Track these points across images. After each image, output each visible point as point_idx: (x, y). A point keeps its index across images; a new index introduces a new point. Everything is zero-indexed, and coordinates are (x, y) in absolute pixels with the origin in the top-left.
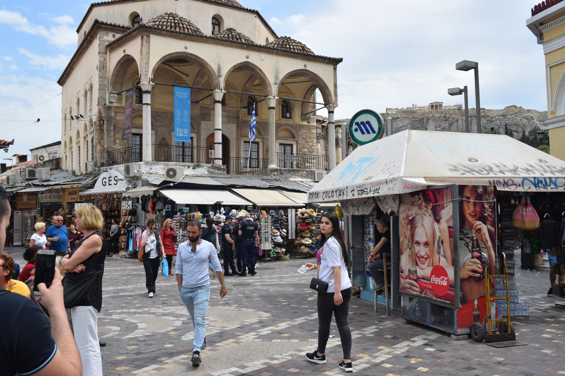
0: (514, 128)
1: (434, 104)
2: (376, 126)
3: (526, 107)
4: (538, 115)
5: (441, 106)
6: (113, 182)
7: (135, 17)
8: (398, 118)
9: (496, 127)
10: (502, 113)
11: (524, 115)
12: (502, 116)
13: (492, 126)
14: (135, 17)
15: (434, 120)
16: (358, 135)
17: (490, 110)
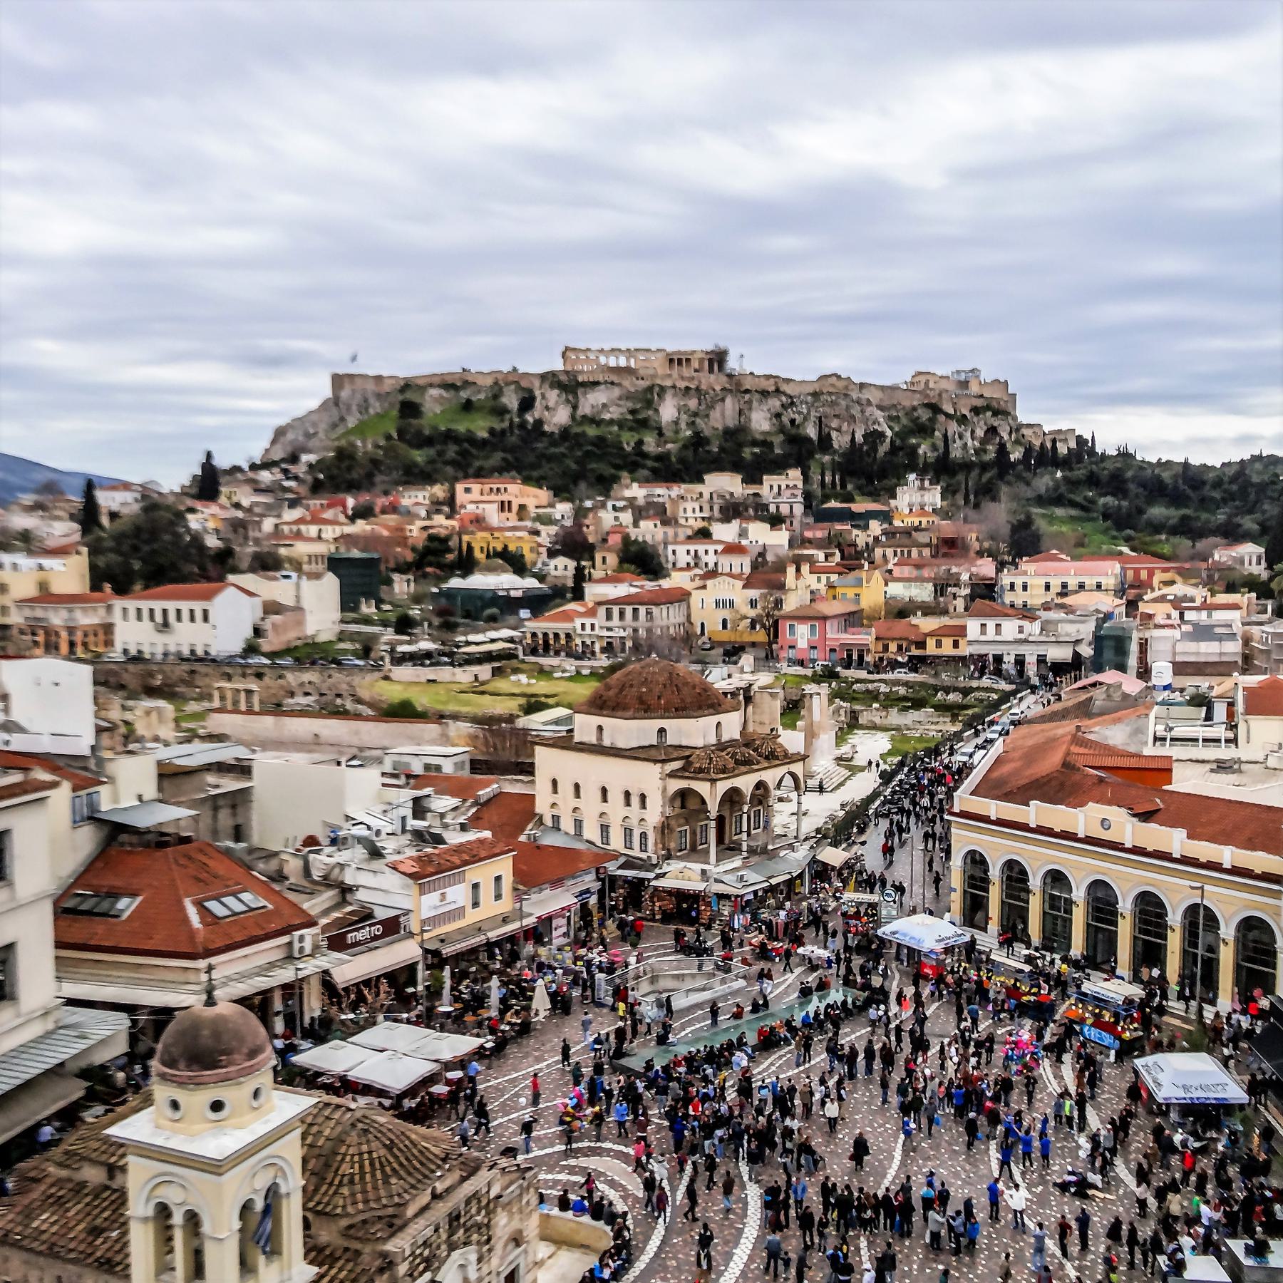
0: (834, 424)
5: (688, 360)
7: (662, 731)
9: (799, 419)
10: (810, 389)
11: (855, 395)
13: (792, 416)
14: (662, 731)
17: (788, 381)
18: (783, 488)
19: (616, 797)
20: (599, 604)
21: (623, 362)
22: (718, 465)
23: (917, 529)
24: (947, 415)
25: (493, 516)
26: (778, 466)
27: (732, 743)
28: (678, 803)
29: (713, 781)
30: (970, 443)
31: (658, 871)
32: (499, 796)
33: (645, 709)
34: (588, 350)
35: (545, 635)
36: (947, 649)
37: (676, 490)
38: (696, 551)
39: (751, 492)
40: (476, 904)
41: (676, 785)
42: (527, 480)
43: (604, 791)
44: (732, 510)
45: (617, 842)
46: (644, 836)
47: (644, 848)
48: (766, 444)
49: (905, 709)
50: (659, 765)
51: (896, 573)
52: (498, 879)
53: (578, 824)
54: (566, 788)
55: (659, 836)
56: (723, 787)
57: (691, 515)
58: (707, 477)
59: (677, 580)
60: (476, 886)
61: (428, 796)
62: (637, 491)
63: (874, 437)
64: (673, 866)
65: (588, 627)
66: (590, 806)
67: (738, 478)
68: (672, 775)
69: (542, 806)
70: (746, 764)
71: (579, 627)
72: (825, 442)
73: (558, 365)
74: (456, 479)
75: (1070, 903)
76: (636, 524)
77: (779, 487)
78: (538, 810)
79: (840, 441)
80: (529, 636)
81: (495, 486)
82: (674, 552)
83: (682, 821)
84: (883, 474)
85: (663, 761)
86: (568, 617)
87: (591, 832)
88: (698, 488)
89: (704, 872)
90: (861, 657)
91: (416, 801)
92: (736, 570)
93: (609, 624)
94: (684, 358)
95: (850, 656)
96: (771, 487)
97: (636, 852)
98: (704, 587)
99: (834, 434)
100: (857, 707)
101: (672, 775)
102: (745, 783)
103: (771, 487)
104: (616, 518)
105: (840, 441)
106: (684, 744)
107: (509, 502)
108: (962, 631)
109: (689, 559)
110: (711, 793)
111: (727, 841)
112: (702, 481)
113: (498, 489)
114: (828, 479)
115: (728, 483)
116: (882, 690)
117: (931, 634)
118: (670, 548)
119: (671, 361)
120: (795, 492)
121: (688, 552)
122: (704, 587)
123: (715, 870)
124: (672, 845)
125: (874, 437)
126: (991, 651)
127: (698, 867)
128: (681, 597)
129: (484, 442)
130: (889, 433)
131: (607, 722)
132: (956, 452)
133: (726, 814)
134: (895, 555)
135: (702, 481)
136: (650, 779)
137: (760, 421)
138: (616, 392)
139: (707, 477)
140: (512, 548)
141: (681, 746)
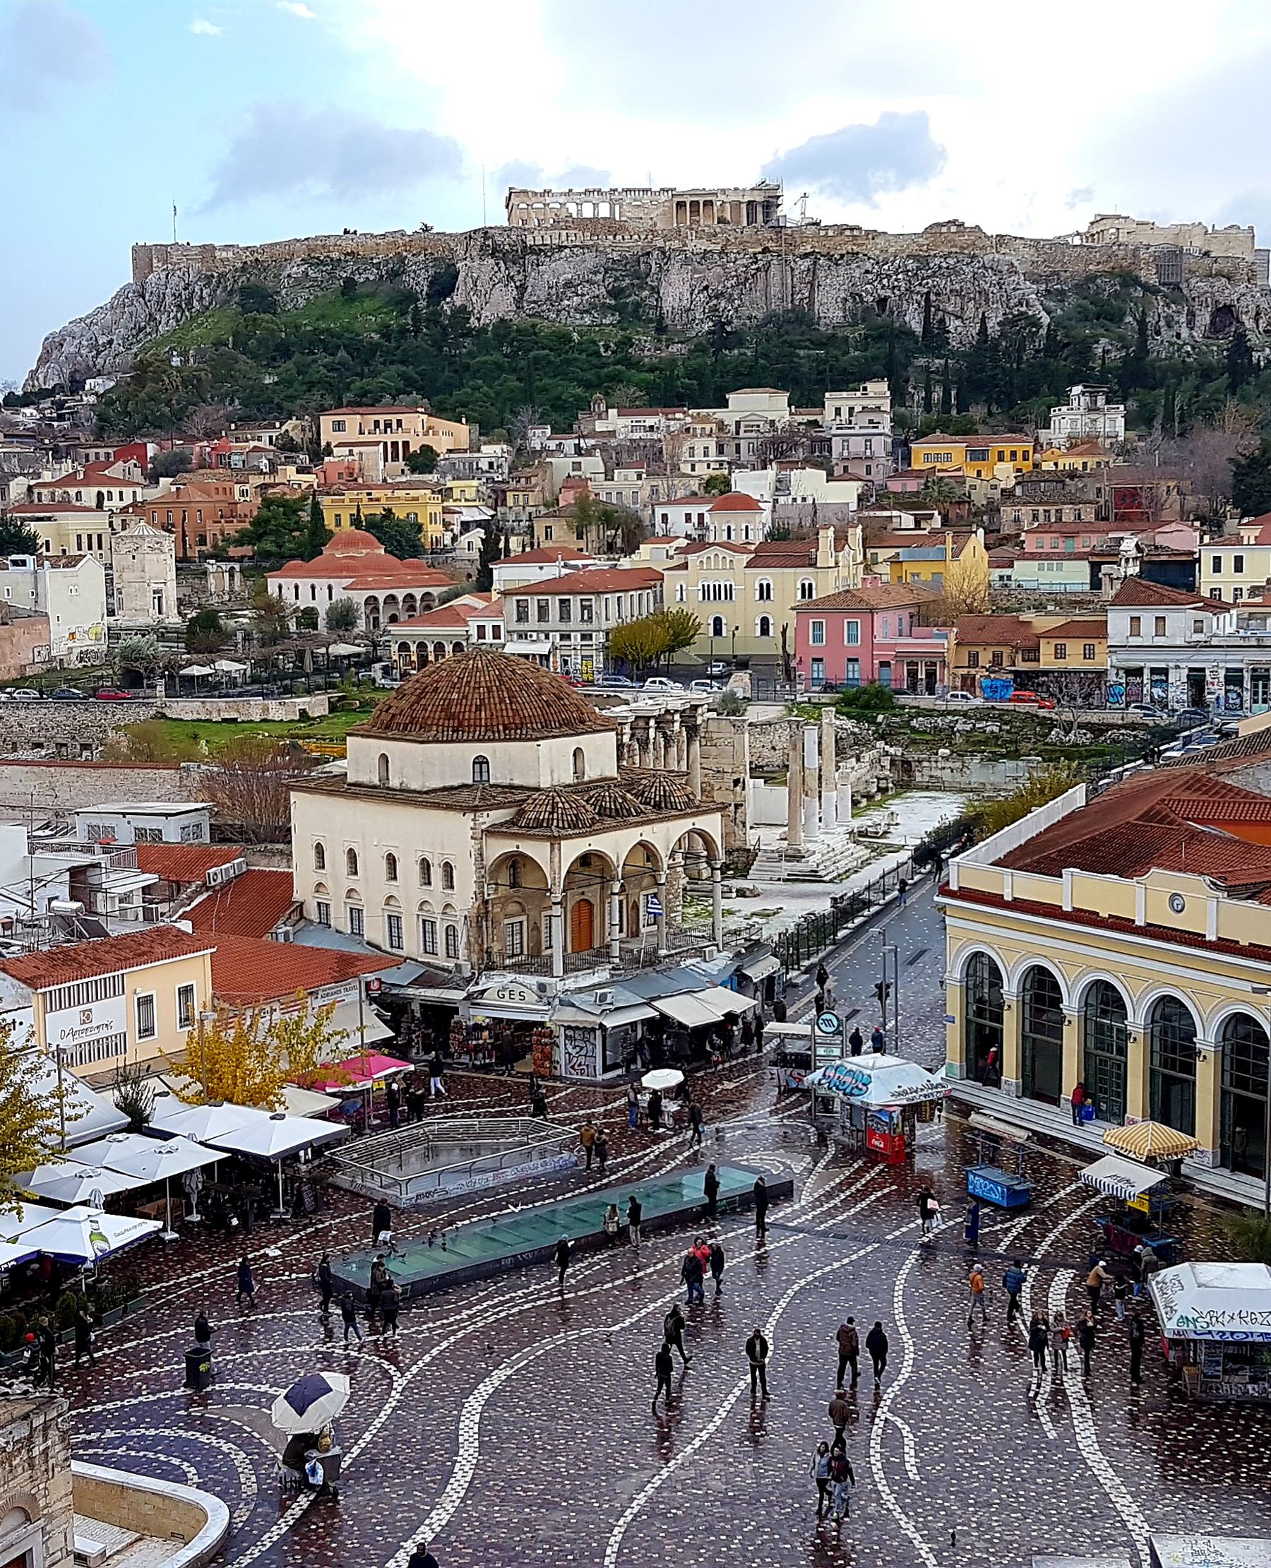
1: (688, 200)
2: (836, 1023)
3: (991, 230)
4: (1029, 254)
5: (709, 204)
6: (517, 997)
7: (481, 762)
8: (561, 248)
12: (915, 257)
14: (481, 762)
15: (687, 261)
16: (823, 1027)
17: (874, 234)
18: (860, 414)
19: (409, 870)
20: (505, 594)
21: (604, 211)
22: (750, 379)
23: (1072, 475)
24: (1147, 288)
25: (376, 464)
26: (850, 379)
27: (602, 782)
28: (504, 878)
29: (554, 840)
30: (1185, 333)
31: (471, 988)
32: (243, 879)
33: (456, 727)
34: (547, 192)
35: (422, 646)
36: (1075, 661)
37: (682, 418)
38: (701, 516)
39: (806, 418)
40: (146, 1031)
41: (498, 848)
42: (439, 411)
43: (392, 861)
44: (776, 450)
45: (412, 944)
46: (451, 931)
47: (451, 952)
48: (830, 341)
49: (995, 758)
50: (472, 816)
51: (1028, 548)
52: (186, 992)
53: (356, 915)
54: (336, 859)
55: (473, 932)
56: (572, 849)
57: (700, 457)
58: (731, 397)
59: (645, 555)
60: (146, 1002)
61: (97, 866)
62: (615, 422)
63: (1019, 322)
64: (493, 983)
65: (489, 632)
66: (372, 886)
67: (783, 398)
68: (491, 832)
69: (302, 890)
70: (617, 816)
71: (474, 632)
72: (934, 337)
73: (498, 217)
74: (323, 410)
75: (1124, 1035)
76: (609, 476)
77: (851, 409)
78: (297, 896)
79: (960, 332)
80: (395, 648)
81: (382, 419)
82: (665, 517)
83: (513, 908)
84: (1030, 390)
85: (475, 809)
86: (457, 618)
87: (376, 931)
88: (719, 414)
89: (542, 988)
90: (931, 675)
91: (77, 874)
92: (738, 538)
93: (523, 627)
94: (701, 200)
95: (913, 674)
96: (838, 411)
97: (441, 960)
98: (685, 566)
99: (953, 324)
100: (913, 756)
101: (491, 832)
102: (616, 844)
103: (838, 411)
104: (577, 466)
105: (960, 332)
106: (516, 782)
107: (406, 444)
108: (1101, 630)
109: (690, 528)
110: (555, 859)
111: (596, 945)
112: (724, 404)
113: (388, 425)
114: (937, 395)
115: (764, 407)
116: (959, 726)
117: (1049, 634)
118: (659, 511)
119: (680, 205)
120: (875, 417)
121: (688, 517)
122: (685, 566)
123: (560, 984)
124: (496, 947)
125: (1019, 322)
126: (1148, 662)
127: (532, 980)
128: (650, 579)
129: (375, 347)
130: (1046, 320)
131: (394, 749)
132: (1159, 347)
133: (592, 894)
134: (1035, 518)
135: (724, 404)
136: (455, 837)
137: (830, 307)
138: (591, 260)
139: (731, 397)
140: (400, 513)
141: (511, 787)
